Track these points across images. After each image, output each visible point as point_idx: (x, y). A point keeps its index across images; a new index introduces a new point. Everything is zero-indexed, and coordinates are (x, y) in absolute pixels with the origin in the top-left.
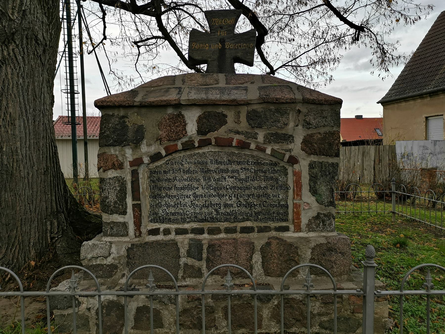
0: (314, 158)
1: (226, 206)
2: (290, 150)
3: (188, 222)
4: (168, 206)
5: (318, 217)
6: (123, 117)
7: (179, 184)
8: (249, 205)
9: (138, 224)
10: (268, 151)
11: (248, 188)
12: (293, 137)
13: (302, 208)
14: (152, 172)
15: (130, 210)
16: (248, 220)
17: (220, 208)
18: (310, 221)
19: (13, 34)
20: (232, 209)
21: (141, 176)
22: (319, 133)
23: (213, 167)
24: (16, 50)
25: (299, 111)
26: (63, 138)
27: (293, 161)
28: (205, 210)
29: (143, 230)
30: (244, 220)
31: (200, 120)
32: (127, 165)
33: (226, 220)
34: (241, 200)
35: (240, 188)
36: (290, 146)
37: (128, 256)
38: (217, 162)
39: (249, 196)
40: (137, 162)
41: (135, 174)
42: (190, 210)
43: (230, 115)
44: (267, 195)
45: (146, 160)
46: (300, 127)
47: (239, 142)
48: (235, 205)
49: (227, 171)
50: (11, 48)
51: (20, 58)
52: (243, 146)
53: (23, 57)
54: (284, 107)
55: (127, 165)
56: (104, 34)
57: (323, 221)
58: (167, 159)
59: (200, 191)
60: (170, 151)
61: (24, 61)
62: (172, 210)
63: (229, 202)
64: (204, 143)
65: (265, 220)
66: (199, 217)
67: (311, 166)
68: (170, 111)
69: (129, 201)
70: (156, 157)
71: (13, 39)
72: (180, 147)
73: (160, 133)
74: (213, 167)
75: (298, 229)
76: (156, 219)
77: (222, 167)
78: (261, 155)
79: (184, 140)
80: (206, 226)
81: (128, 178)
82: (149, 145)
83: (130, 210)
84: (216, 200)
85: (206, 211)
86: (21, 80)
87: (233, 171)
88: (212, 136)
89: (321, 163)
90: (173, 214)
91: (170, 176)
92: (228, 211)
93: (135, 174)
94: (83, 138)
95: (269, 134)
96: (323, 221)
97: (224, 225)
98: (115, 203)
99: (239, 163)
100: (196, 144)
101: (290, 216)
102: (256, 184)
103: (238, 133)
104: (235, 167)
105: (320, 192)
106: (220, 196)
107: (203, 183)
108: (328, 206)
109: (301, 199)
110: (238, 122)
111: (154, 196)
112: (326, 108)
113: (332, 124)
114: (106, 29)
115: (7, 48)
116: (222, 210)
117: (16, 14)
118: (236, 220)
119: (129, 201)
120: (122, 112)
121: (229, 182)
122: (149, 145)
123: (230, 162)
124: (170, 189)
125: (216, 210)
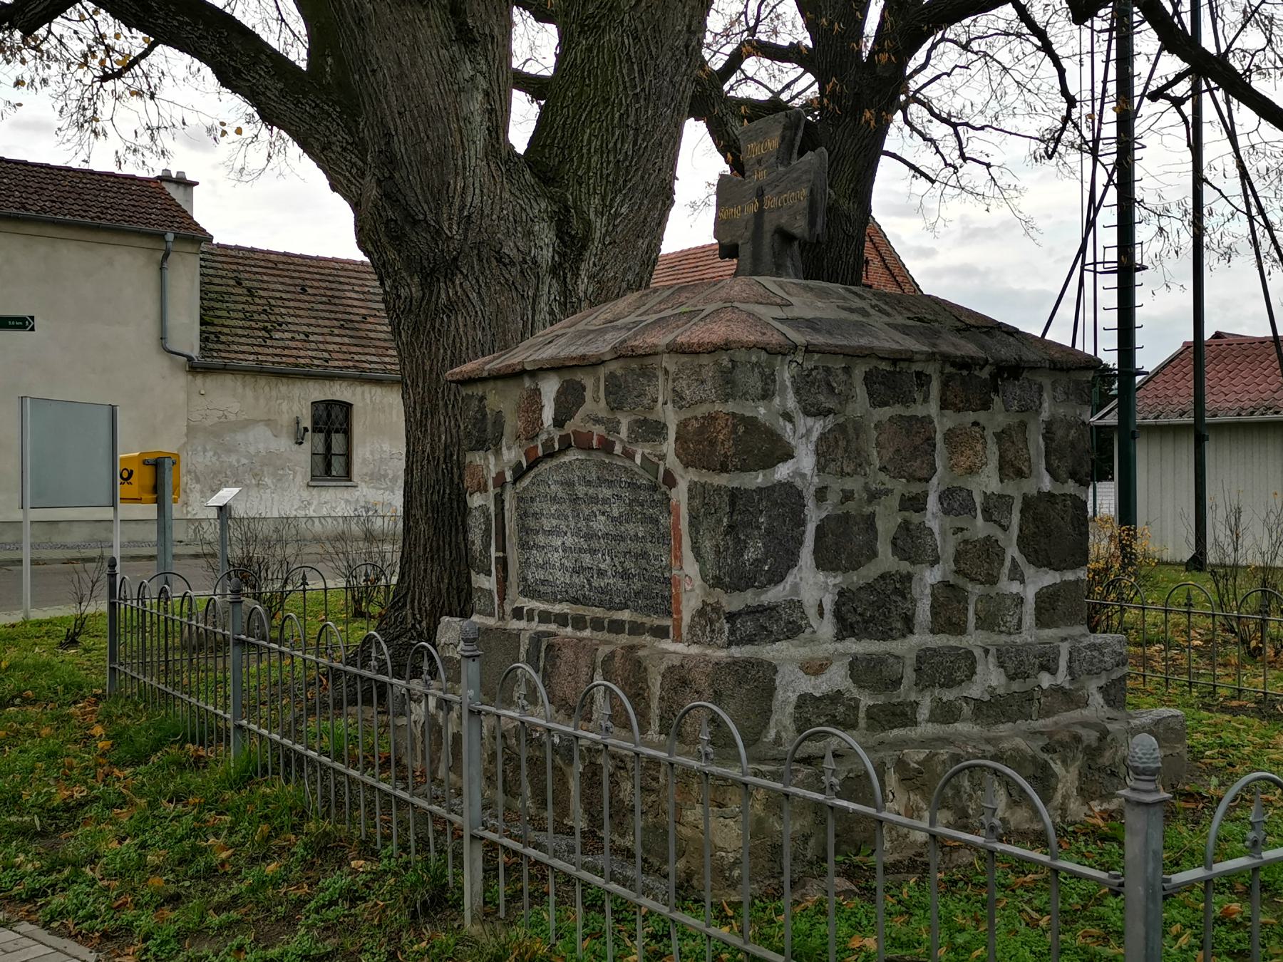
0: (693, 475)
1: (601, 573)
3: (561, 601)
5: (701, 613)
9: (503, 597)
11: (622, 538)
14: (520, 499)
17: (592, 577)
19: (455, 259)
21: (507, 506)
23: (581, 490)
24: (467, 285)
25: (666, 372)
26: (1162, 421)
29: (508, 609)
32: (490, 482)
35: (614, 538)
38: (588, 483)
40: (500, 482)
41: (499, 500)
42: (561, 578)
43: (588, 382)
44: (644, 555)
46: (670, 405)
47: (602, 440)
49: (594, 500)
50: (457, 282)
51: (474, 296)
53: (479, 293)
54: (649, 361)
55: (490, 482)
56: (1064, 91)
58: (532, 474)
59: (569, 540)
61: (482, 300)
62: (541, 575)
63: (603, 566)
64: (566, 445)
66: (572, 593)
68: (527, 383)
71: (457, 268)
74: (581, 490)
75: (678, 638)
76: (529, 592)
77: (591, 491)
79: (544, 437)
81: (492, 508)
82: (509, 448)
86: (480, 333)
88: (570, 427)
89: (703, 486)
90: (544, 582)
93: (499, 500)
94: (1191, 420)
95: (636, 421)
99: (610, 484)
103: (597, 421)
104: (606, 492)
106: (593, 552)
110: (596, 400)
111: (524, 546)
112: (705, 359)
114: (1067, 74)
115: (453, 283)
117: (455, 227)
120: (478, 390)
122: (509, 448)
123: (602, 481)
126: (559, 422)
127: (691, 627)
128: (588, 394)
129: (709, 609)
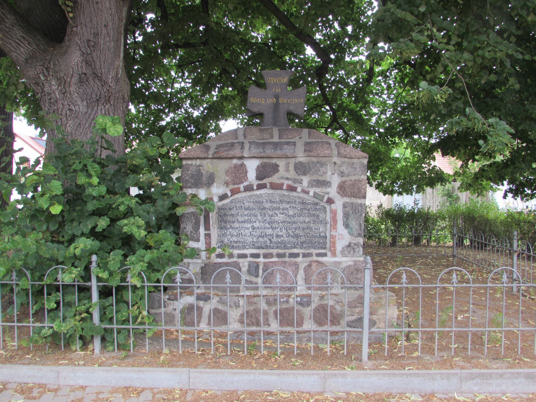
0: (347, 200)
1: (278, 236)
2: (328, 193)
3: (248, 249)
4: (232, 236)
5: (349, 246)
6: (199, 166)
7: (241, 219)
8: (297, 236)
10: (311, 194)
12: (331, 183)
13: (337, 238)
15: (202, 238)
16: (295, 247)
18: (343, 248)
20: (282, 239)
22: (351, 180)
23: (268, 205)
25: (335, 163)
27: (330, 201)
28: (261, 239)
30: (291, 248)
31: (258, 169)
33: (278, 248)
34: (290, 232)
35: (289, 223)
36: (329, 190)
37: (202, 273)
38: (271, 202)
39: (296, 229)
45: (216, 199)
46: (336, 175)
48: (285, 236)
49: (279, 209)
50: (107, 107)
52: (292, 189)
57: (354, 249)
59: (257, 225)
60: (234, 192)
62: (235, 239)
63: (280, 234)
65: (309, 248)
66: (256, 245)
67: (344, 206)
68: (235, 161)
69: (202, 231)
70: (223, 197)
72: (242, 189)
73: (227, 178)
74: (268, 205)
77: (275, 205)
78: (305, 196)
79: (246, 184)
80: (261, 252)
83: (202, 238)
84: (269, 232)
85: (262, 240)
87: (283, 209)
89: (352, 204)
90: (236, 242)
91: (233, 212)
92: (279, 240)
95: (312, 180)
96: (354, 249)
97: (275, 251)
98: (191, 232)
99: (288, 203)
100: (255, 188)
101: (328, 245)
102: (301, 219)
103: (288, 179)
105: (351, 226)
107: (260, 218)
108: (357, 237)
109: (336, 231)
110: (287, 170)
113: (361, 173)
116: (275, 240)
118: (285, 247)
119: (202, 231)
121: (281, 217)
123: (281, 202)
124: (234, 222)
125: (270, 240)
126: (259, 178)
127: (342, 252)
128: (281, 168)
129: (352, 245)
